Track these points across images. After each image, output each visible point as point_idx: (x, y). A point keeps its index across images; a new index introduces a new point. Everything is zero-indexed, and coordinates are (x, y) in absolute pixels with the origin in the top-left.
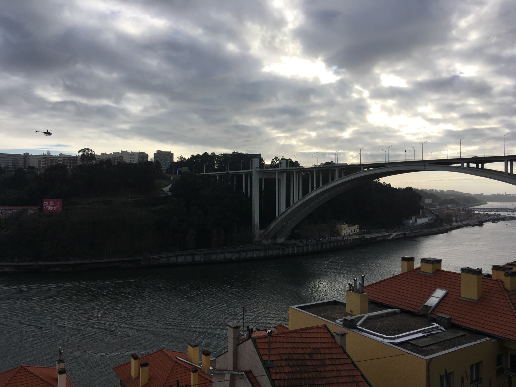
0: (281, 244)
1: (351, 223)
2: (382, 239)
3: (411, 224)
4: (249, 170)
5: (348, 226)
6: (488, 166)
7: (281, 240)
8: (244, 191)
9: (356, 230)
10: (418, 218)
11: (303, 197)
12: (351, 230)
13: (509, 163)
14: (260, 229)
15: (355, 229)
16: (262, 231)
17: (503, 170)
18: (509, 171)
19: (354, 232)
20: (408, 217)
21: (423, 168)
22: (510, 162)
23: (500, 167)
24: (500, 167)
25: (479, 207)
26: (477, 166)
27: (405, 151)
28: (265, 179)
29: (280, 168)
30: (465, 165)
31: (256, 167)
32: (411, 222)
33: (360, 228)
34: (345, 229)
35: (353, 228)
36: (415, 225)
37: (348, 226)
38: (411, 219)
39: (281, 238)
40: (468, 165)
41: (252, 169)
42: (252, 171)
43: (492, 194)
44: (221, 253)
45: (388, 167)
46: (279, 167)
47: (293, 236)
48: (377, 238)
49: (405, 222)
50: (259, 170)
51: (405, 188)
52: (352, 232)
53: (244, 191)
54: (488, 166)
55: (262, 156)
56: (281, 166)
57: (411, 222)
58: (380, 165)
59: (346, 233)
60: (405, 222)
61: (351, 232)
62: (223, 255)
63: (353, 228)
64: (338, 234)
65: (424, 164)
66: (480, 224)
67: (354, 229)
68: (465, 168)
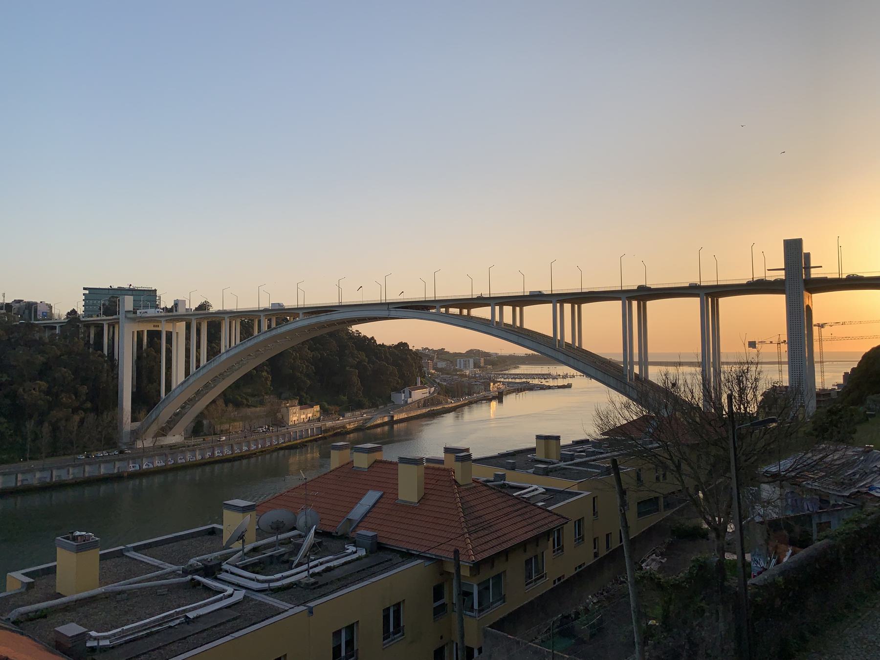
0: (172, 447)
1: (304, 404)
2: (356, 425)
4: (114, 317)
5: (301, 409)
6: (476, 312)
7: (174, 438)
8: (106, 352)
11: (210, 361)
13: (497, 308)
14: (134, 419)
16: (137, 424)
17: (489, 318)
18: (497, 319)
20: (398, 390)
21: (385, 314)
22: (498, 307)
23: (483, 312)
24: (483, 312)
25: (507, 372)
26: (461, 312)
27: (361, 287)
28: (148, 331)
29: (175, 313)
30: (443, 310)
31: (126, 311)
33: (324, 411)
36: (410, 400)
37: (301, 409)
39: (174, 436)
40: (447, 311)
41: (119, 314)
42: (119, 319)
43: (526, 354)
44: (42, 470)
46: (173, 312)
47: (197, 430)
49: (394, 396)
50: (131, 315)
51: (397, 344)
53: (106, 352)
54: (476, 312)
55: (158, 294)
56: (176, 311)
58: (331, 309)
60: (394, 396)
62: (46, 474)
64: (280, 422)
65: (388, 308)
66: (499, 398)
68: (442, 314)
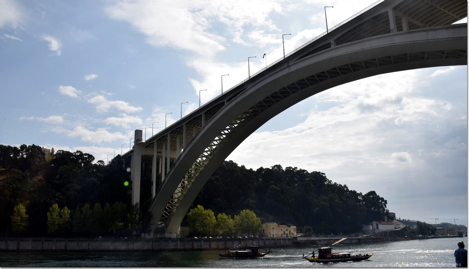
3: (371, 230)
9: (291, 232)
10: (380, 223)
12: (284, 232)
15: (290, 232)
19: (288, 235)
32: (371, 228)
34: (273, 229)
35: (287, 230)
36: (377, 231)
38: (372, 225)
45: (243, 91)
48: (318, 241)
52: (286, 235)
57: (371, 228)
59: (276, 235)
61: (284, 234)
63: (287, 230)
67: (288, 231)
